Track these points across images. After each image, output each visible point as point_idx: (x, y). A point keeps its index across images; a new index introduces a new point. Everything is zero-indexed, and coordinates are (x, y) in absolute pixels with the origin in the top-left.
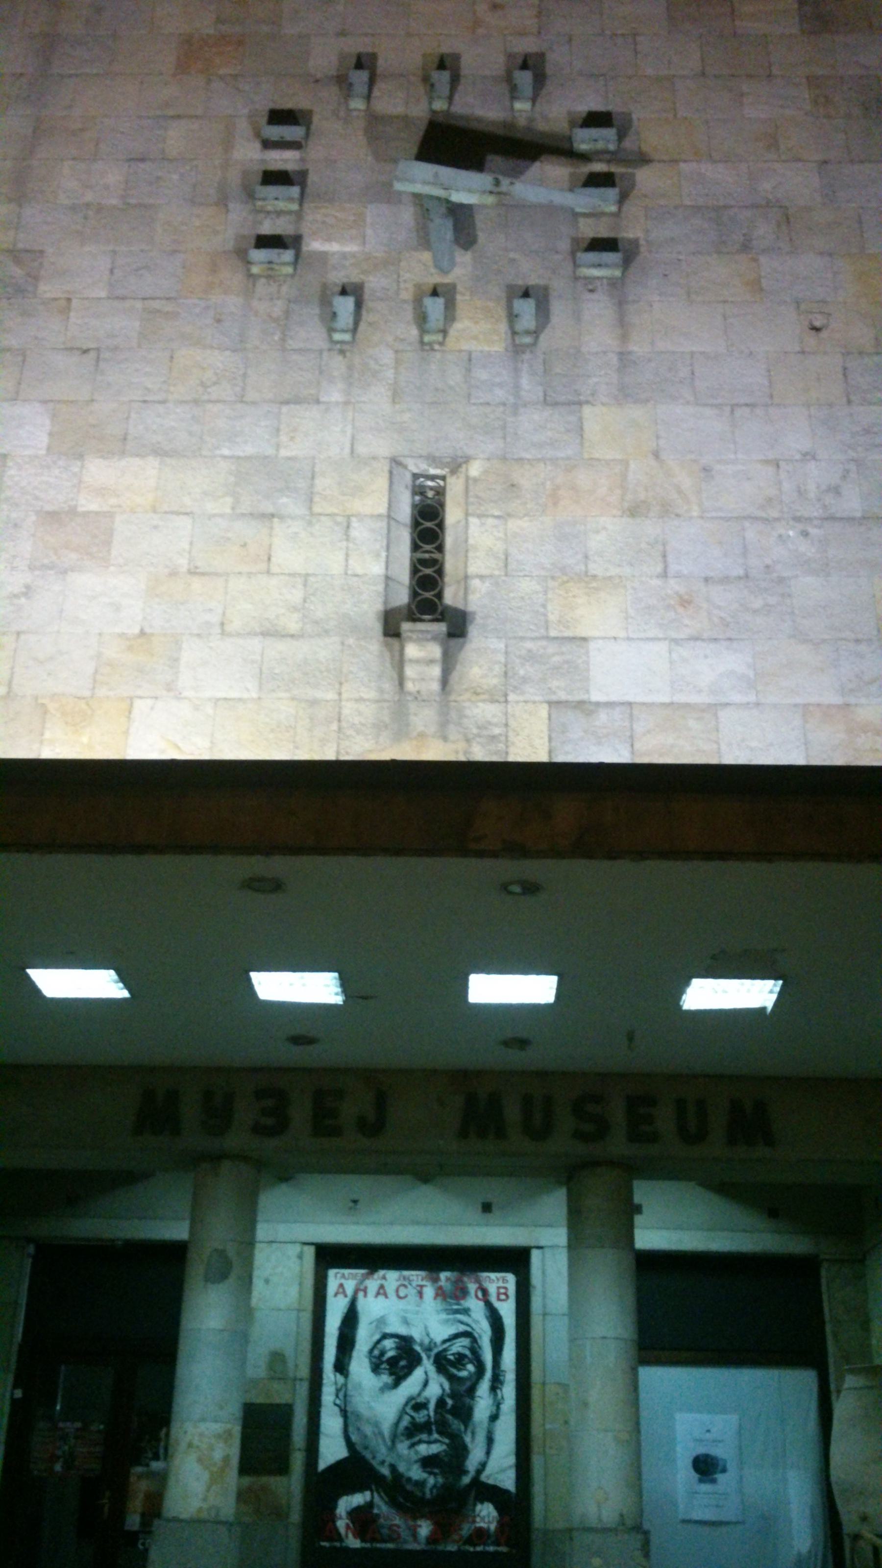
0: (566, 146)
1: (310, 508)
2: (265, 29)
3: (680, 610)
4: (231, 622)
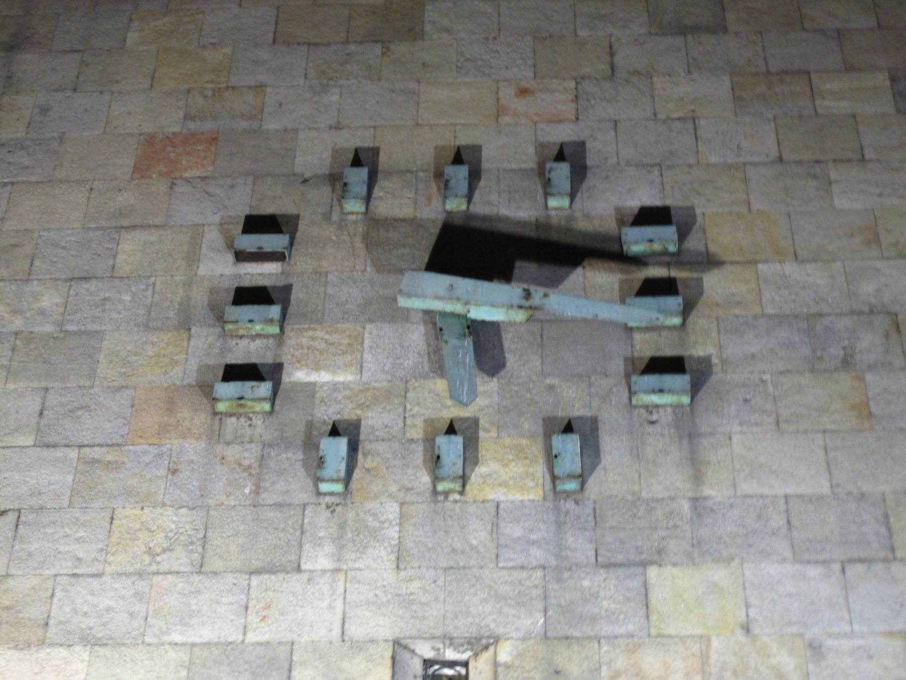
0: (615, 248)
2: (244, 124)
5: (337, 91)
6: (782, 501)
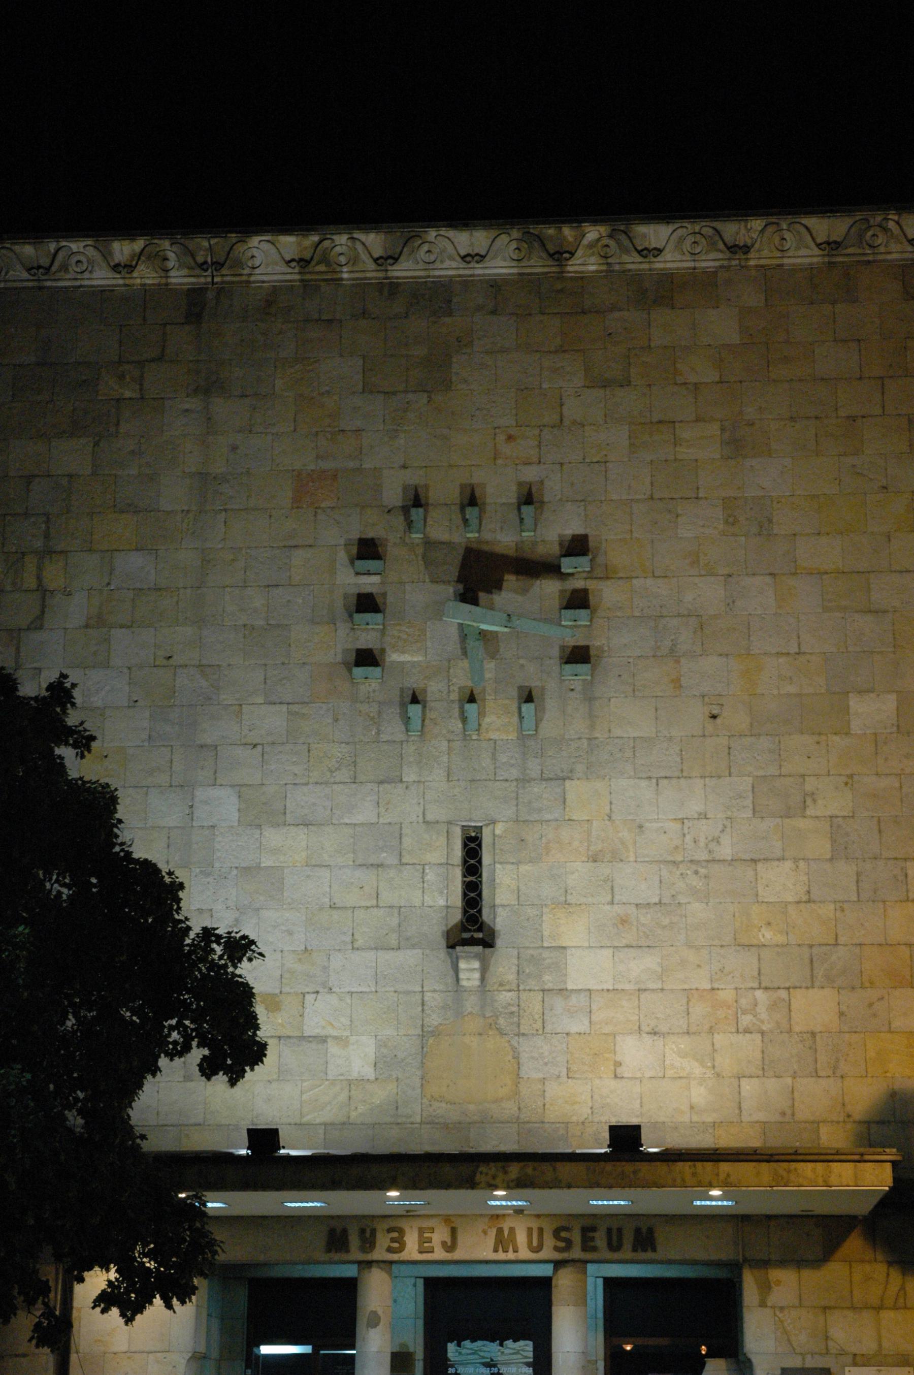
1: (401, 860)
3: (620, 926)
4: (357, 941)
5: (402, 435)
6: (632, 741)
